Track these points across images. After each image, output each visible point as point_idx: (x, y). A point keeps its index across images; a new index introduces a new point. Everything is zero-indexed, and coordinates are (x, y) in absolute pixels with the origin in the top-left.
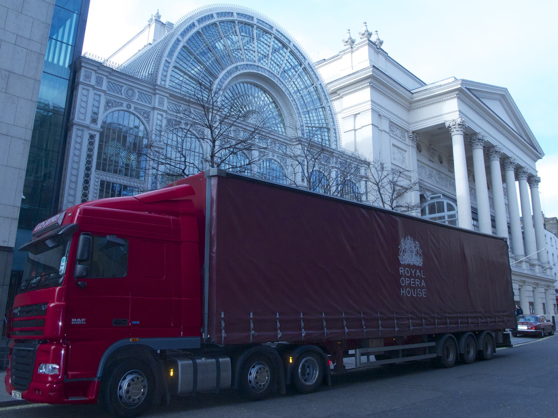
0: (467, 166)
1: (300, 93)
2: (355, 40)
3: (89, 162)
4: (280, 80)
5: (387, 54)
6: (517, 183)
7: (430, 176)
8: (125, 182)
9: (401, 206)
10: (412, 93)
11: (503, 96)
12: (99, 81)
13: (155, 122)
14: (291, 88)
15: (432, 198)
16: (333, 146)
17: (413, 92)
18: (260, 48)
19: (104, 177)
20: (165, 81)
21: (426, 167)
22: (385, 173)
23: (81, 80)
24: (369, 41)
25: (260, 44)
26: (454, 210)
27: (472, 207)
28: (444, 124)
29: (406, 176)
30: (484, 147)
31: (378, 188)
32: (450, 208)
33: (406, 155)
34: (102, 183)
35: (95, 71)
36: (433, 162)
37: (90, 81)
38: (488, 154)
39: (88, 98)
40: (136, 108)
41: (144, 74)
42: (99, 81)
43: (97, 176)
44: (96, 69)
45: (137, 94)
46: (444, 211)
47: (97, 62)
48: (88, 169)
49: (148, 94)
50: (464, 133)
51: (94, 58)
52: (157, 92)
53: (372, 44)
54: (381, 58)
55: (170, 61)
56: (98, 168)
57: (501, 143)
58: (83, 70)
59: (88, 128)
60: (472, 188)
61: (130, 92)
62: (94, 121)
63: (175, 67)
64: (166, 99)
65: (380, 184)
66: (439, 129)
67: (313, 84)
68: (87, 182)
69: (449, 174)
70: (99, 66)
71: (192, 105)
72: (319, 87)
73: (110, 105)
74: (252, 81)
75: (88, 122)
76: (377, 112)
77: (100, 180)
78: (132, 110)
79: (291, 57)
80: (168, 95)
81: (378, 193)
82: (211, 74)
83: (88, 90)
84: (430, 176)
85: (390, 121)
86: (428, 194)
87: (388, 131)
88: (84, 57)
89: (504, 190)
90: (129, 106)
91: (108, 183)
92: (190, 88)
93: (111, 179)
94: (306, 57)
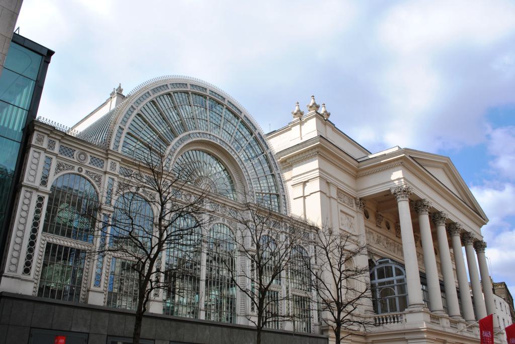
0: (414, 232)
1: (251, 161)
2: (303, 112)
3: (36, 224)
4: (231, 148)
5: (334, 125)
6: (464, 248)
7: (378, 242)
8: (73, 245)
9: (350, 271)
10: (359, 162)
11: (446, 164)
12: (51, 145)
13: (106, 186)
14: (242, 156)
15: (380, 263)
16: (283, 212)
17: (359, 160)
18: (212, 118)
19: (51, 240)
20: (117, 147)
21: (374, 232)
22: (333, 238)
23: (33, 143)
24: (317, 112)
25: (212, 114)
26: (403, 274)
27: (420, 272)
28: (389, 191)
29: (353, 240)
30: (429, 213)
31: (326, 252)
32: (399, 273)
33: (355, 221)
34: (49, 245)
35: (48, 135)
36: (380, 228)
37: (42, 144)
38: (434, 219)
39: (38, 161)
40: (87, 172)
41: (98, 140)
42: (51, 145)
43: (44, 238)
44: (49, 133)
45: (89, 158)
46: (392, 276)
47: (51, 126)
48: (35, 231)
49: (101, 158)
50: (409, 199)
51: (47, 122)
52: (109, 156)
53: (319, 116)
54: (329, 129)
55: (123, 127)
56: (45, 230)
57: (446, 210)
58: (35, 133)
59: (37, 190)
60: (419, 254)
61: (82, 156)
62: (44, 183)
63: (128, 134)
64: (118, 164)
65: (328, 248)
66: (385, 195)
67: (263, 153)
68: (32, 244)
69: (397, 239)
70: (51, 131)
71: (143, 170)
72: (269, 155)
73: (61, 168)
74: (204, 148)
75: (37, 184)
76: (325, 180)
77: (46, 242)
78: (83, 173)
79: (242, 126)
80: (120, 160)
81: (326, 257)
82: (164, 141)
83: (39, 153)
84: (378, 242)
85: (338, 188)
86: (377, 258)
87: (336, 198)
88: (38, 122)
89: (451, 256)
90: (80, 170)
91: (55, 245)
92: (145, 155)
93: (58, 241)
94: (256, 127)
